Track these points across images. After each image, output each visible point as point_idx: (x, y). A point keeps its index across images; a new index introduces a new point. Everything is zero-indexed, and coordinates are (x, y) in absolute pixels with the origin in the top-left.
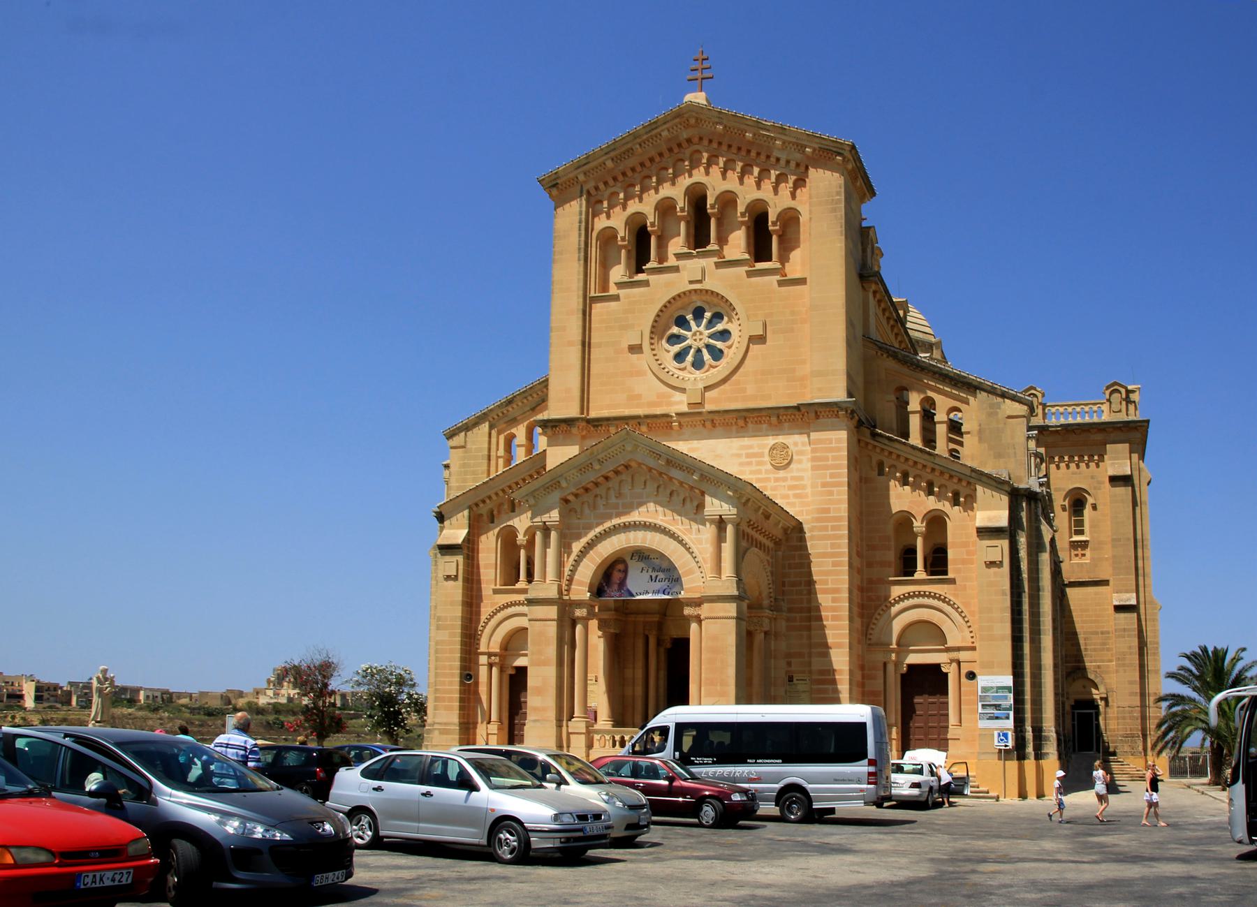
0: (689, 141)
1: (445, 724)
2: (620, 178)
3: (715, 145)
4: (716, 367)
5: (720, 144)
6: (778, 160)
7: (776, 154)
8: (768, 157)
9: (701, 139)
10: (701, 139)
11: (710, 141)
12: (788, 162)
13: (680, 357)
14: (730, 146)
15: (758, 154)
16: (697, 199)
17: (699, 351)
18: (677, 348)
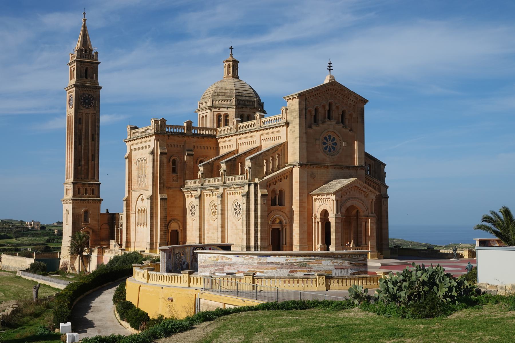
0: (331, 89)
1: (264, 246)
2: (314, 96)
3: (337, 92)
4: (334, 152)
5: (338, 92)
6: (350, 99)
7: (351, 98)
8: (348, 98)
9: (334, 89)
10: (334, 89)
11: (336, 91)
12: (352, 101)
13: (326, 148)
14: (340, 93)
15: (346, 97)
16: (330, 105)
17: (330, 147)
18: (325, 146)
